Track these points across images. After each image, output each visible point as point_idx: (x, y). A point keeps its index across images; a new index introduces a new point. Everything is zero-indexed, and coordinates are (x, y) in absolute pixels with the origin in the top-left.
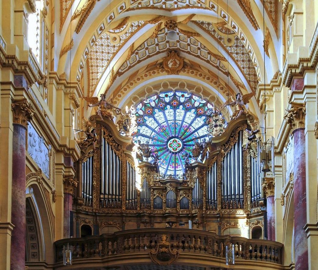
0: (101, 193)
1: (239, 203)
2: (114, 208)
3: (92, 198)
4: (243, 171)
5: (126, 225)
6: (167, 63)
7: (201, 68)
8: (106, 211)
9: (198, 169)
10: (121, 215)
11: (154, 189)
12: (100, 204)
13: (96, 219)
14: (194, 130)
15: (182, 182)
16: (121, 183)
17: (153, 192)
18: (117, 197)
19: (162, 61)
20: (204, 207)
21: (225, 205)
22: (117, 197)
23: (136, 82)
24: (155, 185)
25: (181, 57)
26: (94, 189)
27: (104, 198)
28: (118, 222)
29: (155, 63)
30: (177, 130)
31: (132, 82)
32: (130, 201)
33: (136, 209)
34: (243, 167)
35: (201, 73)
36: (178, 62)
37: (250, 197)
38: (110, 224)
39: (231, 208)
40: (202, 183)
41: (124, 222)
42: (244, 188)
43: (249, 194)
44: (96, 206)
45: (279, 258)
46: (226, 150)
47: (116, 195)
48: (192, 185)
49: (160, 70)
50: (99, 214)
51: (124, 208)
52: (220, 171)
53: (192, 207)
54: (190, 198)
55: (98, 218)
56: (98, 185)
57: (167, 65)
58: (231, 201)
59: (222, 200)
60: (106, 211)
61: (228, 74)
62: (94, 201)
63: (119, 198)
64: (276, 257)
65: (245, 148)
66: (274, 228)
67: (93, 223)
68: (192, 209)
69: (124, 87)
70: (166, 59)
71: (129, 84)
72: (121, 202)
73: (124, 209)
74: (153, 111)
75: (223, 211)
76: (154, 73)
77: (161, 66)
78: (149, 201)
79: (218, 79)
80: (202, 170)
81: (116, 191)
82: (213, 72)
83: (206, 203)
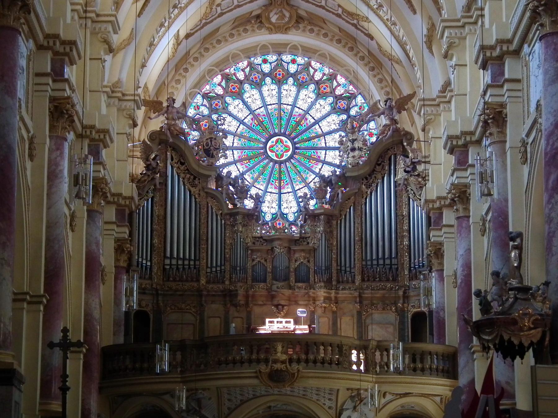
0: (165, 257)
1: (391, 272)
2: (187, 281)
3: (151, 266)
4: (396, 219)
5: (206, 309)
6: (269, 15)
7: (326, 24)
8: (174, 285)
9: (324, 218)
10: (199, 293)
11: (252, 250)
12: (163, 275)
13: (158, 300)
14: (314, 121)
15: (298, 238)
16: (199, 240)
17: (251, 254)
18: (192, 263)
19: (258, 12)
20: (334, 278)
21: (368, 276)
22: (192, 263)
23: (214, 47)
24: (254, 243)
25: (293, 6)
26: (155, 251)
27: (171, 265)
28: (194, 305)
29: (247, 16)
30: (283, 123)
31: (207, 47)
32: (214, 269)
33: (223, 282)
34: (396, 213)
35: (326, 31)
36: (287, 15)
37: (408, 263)
38: (181, 309)
39: (379, 281)
40: (331, 239)
41: (202, 305)
42: (398, 247)
43: (407, 259)
44: (157, 278)
45: (450, 369)
46: (369, 185)
47: (190, 260)
48: (314, 243)
49: (256, 26)
50: (162, 293)
51: (203, 281)
52: (360, 220)
53: (315, 279)
54: (311, 265)
55: (160, 298)
56: (161, 244)
57: (268, 19)
58: (377, 269)
59: (363, 268)
60: (174, 285)
61: (372, 38)
62: (155, 270)
63: (195, 265)
64: (446, 368)
65: (400, 184)
66: (444, 320)
67: (153, 307)
68: (315, 282)
69: (192, 55)
70: (268, 7)
71: (202, 50)
72: (199, 271)
73: (203, 284)
74: (241, 88)
75: (364, 285)
76: (246, 31)
77: (259, 21)
78: (244, 269)
79: (356, 43)
80: (330, 218)
81: (189, 252)
82: (348, 31)
83: (337, 273)
